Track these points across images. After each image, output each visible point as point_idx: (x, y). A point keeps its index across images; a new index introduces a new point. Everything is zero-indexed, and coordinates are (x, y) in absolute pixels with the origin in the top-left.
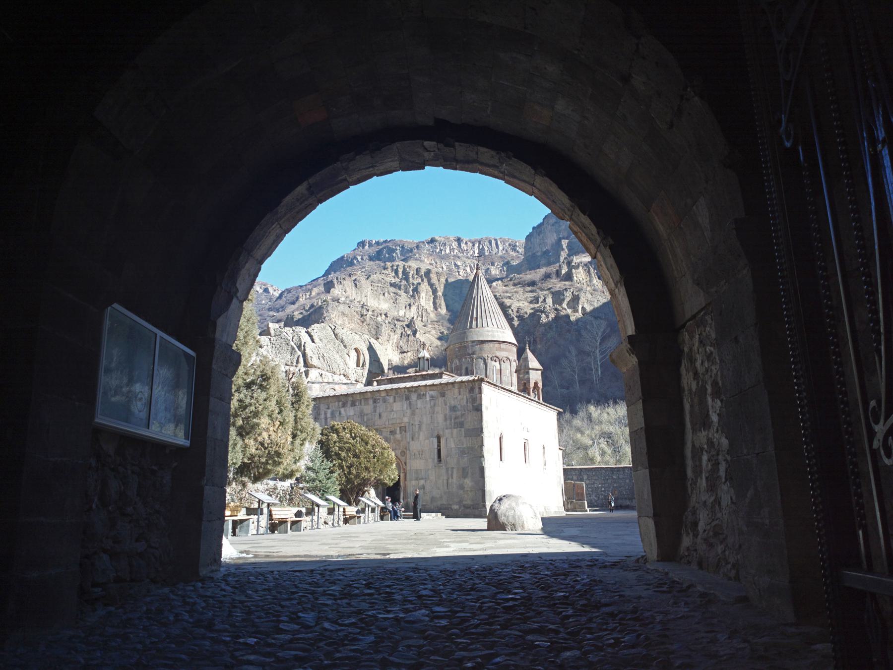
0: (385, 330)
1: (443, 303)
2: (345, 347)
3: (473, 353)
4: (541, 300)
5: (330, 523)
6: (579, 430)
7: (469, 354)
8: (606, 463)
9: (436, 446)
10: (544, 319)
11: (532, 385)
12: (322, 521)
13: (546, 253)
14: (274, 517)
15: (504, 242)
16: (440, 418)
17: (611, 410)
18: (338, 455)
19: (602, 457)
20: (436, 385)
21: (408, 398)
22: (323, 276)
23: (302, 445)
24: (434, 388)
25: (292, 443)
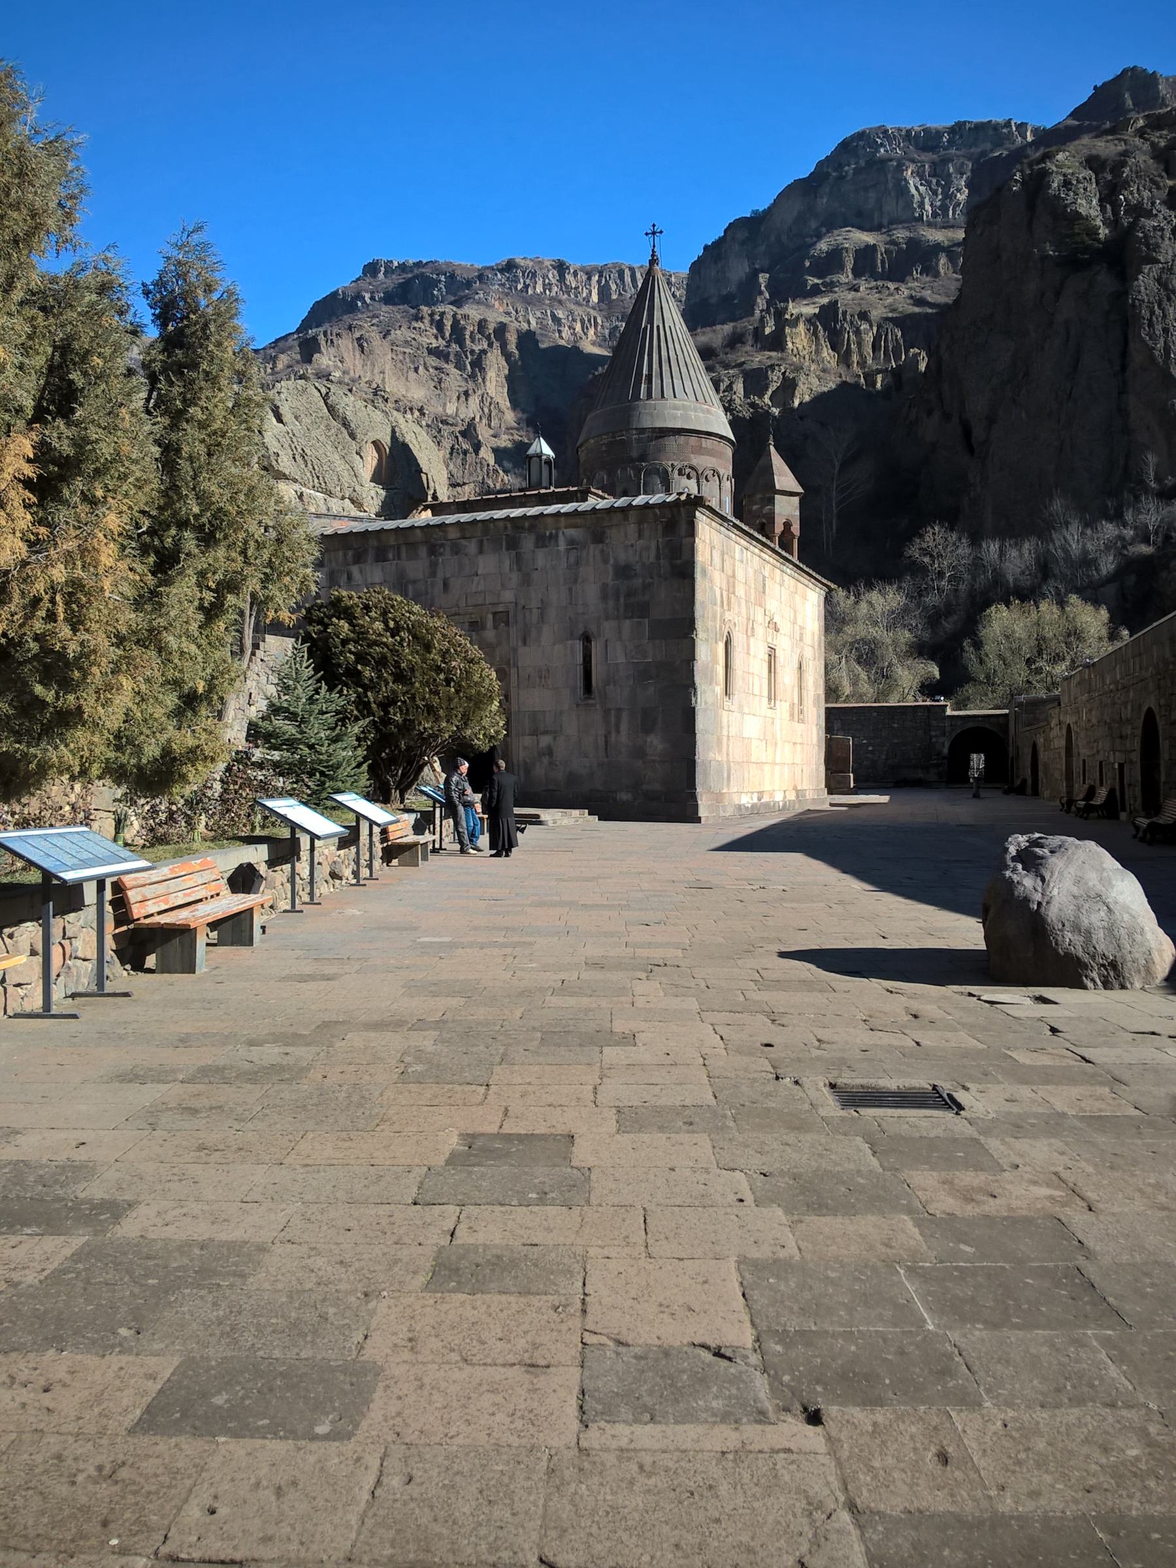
2: (353, 436)
3: (643, 457)
5: (347, 873)
7: (632, 460)
8: (860, 698)
9: (579, 659)
11: (779, 528)
12: (322, 872)
13: (729, 298)
14: (137, 911)
16: (591, 593)
17: (874, 596)
18: (354, 676)
20: (584, 513)
21: (513, 544)
22: (298, 331)
23: (211, 612)
24: (579, 521)
25: (148, 599)
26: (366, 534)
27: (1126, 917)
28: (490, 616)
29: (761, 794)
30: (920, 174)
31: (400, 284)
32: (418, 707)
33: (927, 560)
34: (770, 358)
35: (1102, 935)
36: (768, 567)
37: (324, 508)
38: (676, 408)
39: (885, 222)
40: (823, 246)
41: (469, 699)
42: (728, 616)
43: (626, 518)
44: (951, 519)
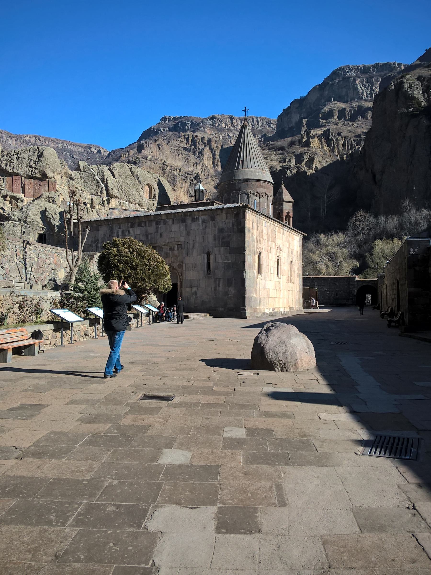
0: (179, 180)
1: (219, 163)
2: (140, 182)
3: (239, 189)
4: (287, 160)
5: (94, 334)
6: (310, 251)
7: (236, 190)
8: (329, 274)
9: (206, 261)
10: (289, 174)
11: (285, 214)
13: (291, 129)
15: (262, 119)
16: (210, 238)
17: (335, 237)
18: (117, 267)
19: (326, 270)
21: (184, 221)
22: (137, 142)
24: (206, 213)
26: (135, 217)
27: (291, 349)
28: (176, 246)
29: (274, 309)
30: (362, 83)
31: (174, 125)
32: (138, 278)
33: (358, 223)
34: (304, 150)
35: (281, 354)
36: (277, 228)
37: (128, 207)
38: (252, 172)
39: (349, 100)
40: (326, 109)
41: (157, 275)
42: (259, 246)
43: (222, 212)
44: (368, 208)
